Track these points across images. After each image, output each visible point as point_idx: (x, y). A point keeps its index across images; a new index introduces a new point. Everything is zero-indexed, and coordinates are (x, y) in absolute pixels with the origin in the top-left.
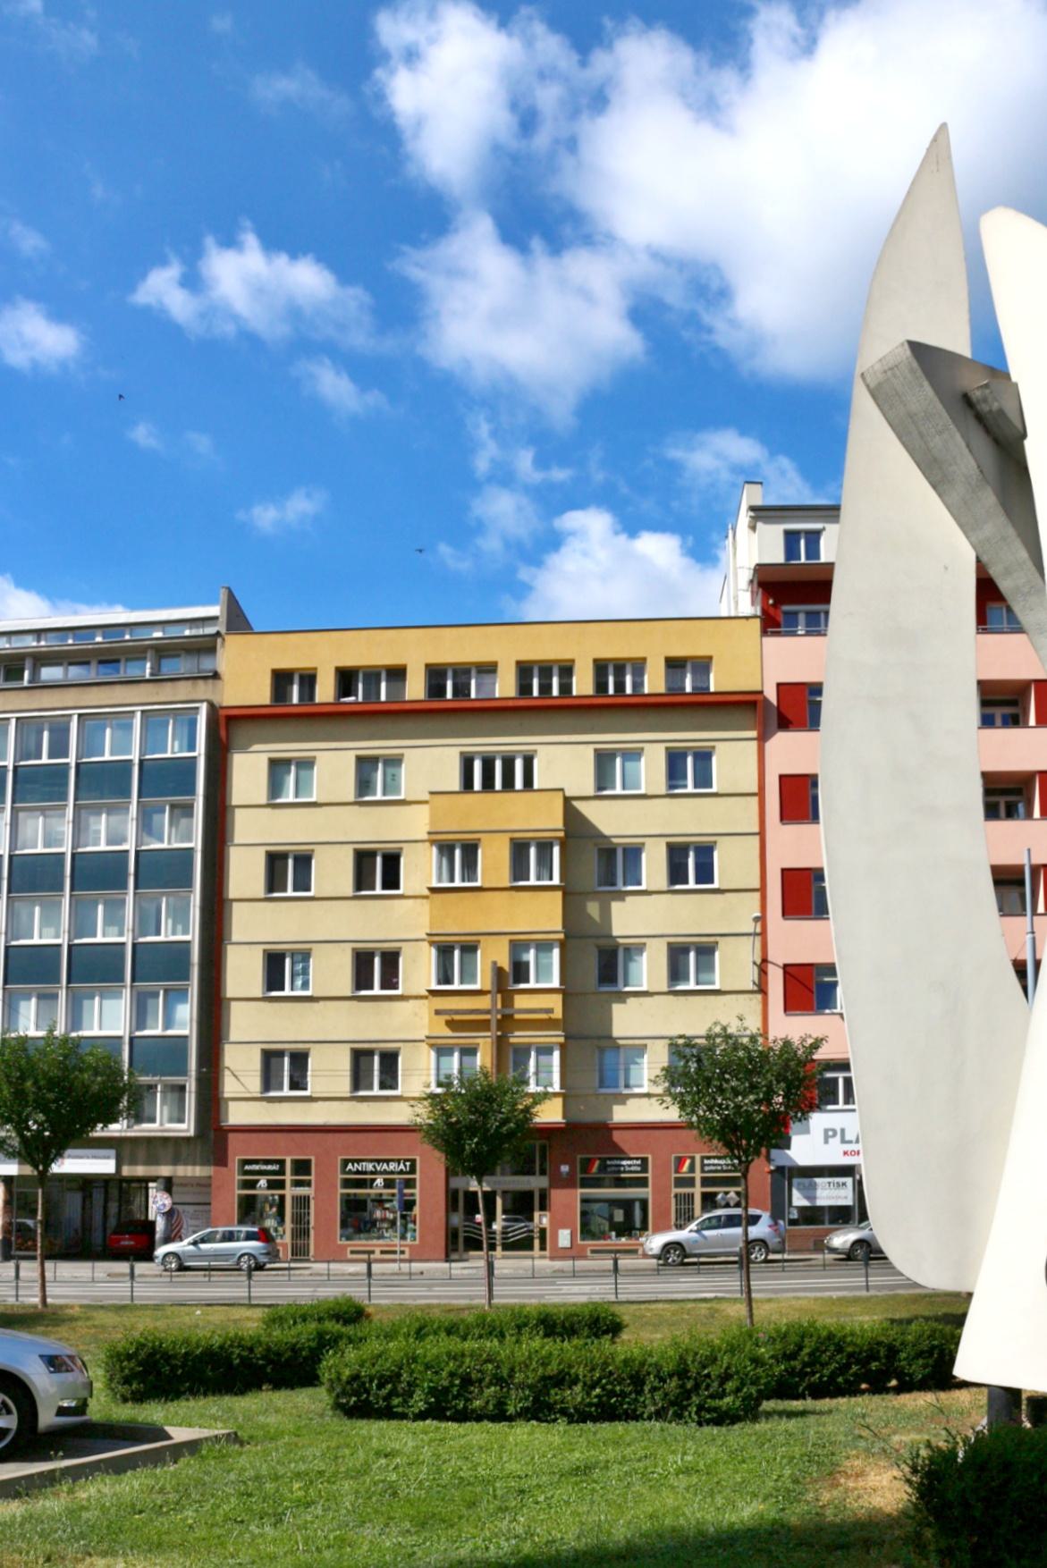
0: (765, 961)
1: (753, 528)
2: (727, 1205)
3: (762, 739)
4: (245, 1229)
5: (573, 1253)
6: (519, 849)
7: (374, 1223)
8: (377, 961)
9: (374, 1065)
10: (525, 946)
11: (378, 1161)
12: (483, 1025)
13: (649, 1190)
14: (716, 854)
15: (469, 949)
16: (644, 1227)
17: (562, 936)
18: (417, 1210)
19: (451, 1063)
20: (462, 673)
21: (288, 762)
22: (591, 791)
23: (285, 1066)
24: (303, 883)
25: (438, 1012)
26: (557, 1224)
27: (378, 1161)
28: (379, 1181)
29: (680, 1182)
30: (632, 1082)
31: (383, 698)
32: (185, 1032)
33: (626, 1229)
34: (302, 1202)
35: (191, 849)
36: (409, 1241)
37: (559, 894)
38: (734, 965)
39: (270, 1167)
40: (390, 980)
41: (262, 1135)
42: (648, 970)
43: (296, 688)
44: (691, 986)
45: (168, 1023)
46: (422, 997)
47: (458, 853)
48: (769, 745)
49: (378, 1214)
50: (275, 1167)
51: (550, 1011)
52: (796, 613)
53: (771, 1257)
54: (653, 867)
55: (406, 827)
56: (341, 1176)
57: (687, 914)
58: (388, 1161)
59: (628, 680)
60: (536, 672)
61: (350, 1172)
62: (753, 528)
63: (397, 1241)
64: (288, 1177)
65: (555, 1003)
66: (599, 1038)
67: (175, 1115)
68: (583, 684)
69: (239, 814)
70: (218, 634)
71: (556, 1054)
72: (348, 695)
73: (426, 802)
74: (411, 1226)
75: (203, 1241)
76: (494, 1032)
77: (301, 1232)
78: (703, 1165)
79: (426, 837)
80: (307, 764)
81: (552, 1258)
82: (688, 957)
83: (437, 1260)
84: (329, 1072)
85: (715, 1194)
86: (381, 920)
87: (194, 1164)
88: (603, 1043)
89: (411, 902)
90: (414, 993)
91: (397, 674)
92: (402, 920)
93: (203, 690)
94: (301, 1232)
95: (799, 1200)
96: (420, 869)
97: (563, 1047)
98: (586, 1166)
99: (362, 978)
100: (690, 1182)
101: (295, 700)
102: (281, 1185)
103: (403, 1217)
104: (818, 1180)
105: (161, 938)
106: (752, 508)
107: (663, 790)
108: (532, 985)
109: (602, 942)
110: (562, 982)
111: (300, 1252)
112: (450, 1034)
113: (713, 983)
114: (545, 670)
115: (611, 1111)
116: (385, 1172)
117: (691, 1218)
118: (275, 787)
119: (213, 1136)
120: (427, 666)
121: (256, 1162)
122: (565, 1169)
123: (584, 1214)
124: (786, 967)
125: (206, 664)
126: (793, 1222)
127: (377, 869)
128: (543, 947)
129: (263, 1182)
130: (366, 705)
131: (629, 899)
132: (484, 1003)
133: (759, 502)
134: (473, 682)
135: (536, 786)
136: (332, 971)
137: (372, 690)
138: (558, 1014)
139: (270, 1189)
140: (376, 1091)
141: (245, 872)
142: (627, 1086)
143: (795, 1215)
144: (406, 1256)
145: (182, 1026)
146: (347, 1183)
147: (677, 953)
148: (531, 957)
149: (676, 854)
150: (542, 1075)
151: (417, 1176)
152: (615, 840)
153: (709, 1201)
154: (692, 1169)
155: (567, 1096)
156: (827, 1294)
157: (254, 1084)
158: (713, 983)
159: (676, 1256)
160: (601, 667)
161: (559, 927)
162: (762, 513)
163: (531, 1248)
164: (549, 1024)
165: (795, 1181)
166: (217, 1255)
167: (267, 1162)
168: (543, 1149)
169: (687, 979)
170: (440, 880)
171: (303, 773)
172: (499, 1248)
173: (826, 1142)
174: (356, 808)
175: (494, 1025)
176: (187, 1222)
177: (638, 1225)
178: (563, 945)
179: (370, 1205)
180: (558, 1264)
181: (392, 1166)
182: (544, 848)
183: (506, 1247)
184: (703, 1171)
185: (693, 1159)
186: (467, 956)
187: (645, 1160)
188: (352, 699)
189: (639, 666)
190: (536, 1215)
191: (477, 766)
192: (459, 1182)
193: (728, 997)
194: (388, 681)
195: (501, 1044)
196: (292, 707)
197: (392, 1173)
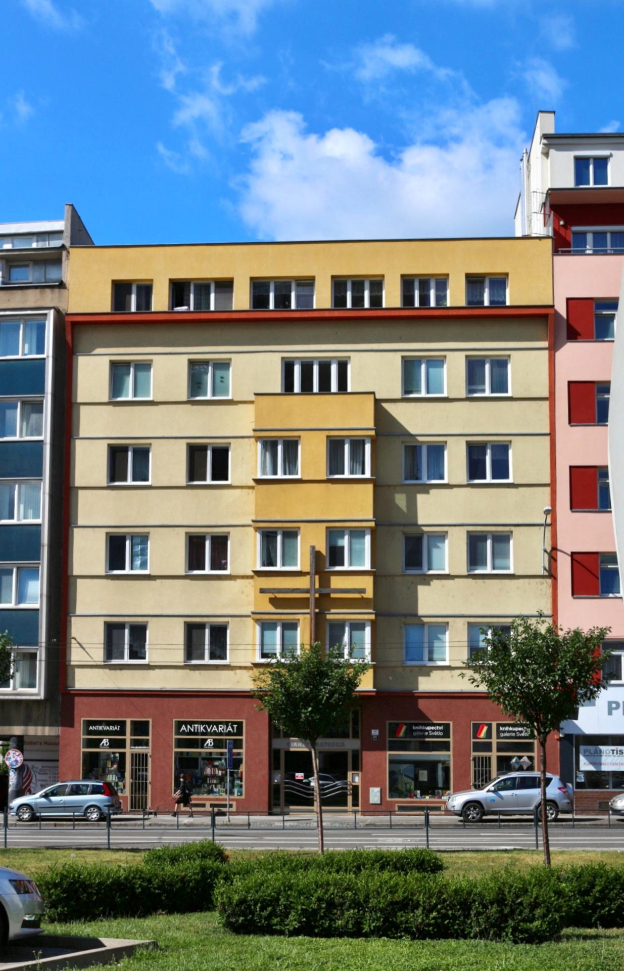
0: (554, 549)
1: (546, 154)
2: (521, 769)
3: (553, 349)
4: (90, 783)
5: (383, 808)
6: (335, 446)
7: (204, 779)
9: (205, 638)
10: (340, 533)
11: (209, 723)
12: (302, 603)
13: (451, 753)
14: (510, 452)
15: (291, 535)
16: (446, 787)
17: (373, 524)
18: (243, 768)
19: (274, 638)
20: (283, 286)
21: (127, 364)
22: (398, 394)
24: (141, 473)
25: (262, 591)
26: (368, 783)
28: (209, 742)
29: (478, 747)
30: (435, 656)
31: (212, 308)
32: (37, 606)
33: (430, 788)
34: (140, 760)
35: (41, 442)
36: (236, 796)
37: (370, 487)
38: (526, 552)
39: (111, 728)
40: (219, 562)
42: (450, 555)
43: (134, 298)
44: (488, 570)
45: (21, 598)
46: (247, 577)
47: (280, 448)
48: (559, 355)
49: (208, 771)
51: (363, 591)
52: (584, 234)
53: (560, 816)
54: (455, 463)
55: (234, 425)
57: (485, 506)
58: (217, 724)
59: (432, 293)
60: (349, 285)
61: (184, 733)
62: (546, 154)
63: (227, 797)
64: (128, 737)
65: (367, 583)
66: (405, 616)
67: (27, 681)
68: (391, 298)
69: (83, 410)
70: (63, 247)
71: (368, 630)
72: (182, 305)
73: (252, 402)
74: (237, 782)
75: (54, 793)
76: (312, 609)
77: (139, 787)
78: (498, 732)
79: (252, 433)
80: (144, 366)
81: (364, 813)
82: (483, 544)
83: (261, 813)
84: (165, 643)
85: (511, 758)
86: (210, 508)
87: (44, 725)
88: (410, 620)
89: (238, 491)
91: (225, 286)
92: (232, 507)
93: (50, 298)
94: (139, 787)
95: (585, 765)
96: (246, 462)
97: (373, 624)
98: (394, 730)
99: (195, 560)
100: (487, 747)
101: (133, 309)
102: (122, 744)
103: (232, 774)
104: (602, 748)
105: (14, 521)
106: (545, 136)
108: (346, 567)
109: (410, 530)
110: (373, 565)
112: (273, 610)
113: (508, 568)
114: (358, 284)
116: (215, 733)
117: (487, 779)
118: (116, 386)
119: (61, 699)
122: (375, 732)
123: (392, 773)
124: (573, 555)
125: (53, 274)
126: (579, 785)
127: (208, 462)
128: (357, 534)
130: (195, 314)
131: (433, 492)
132: (303, 583)
133: (551, 131)
134: (293, 295)
135: (349, 390)
137: (202, 302)
138: (369, 594)
139: (109, 746)
140: (207, 661)
141: (90, 463)
142: (431, 659)
143: (582, 779)
144: (234, 809)
145: (34, 600)
146: (180, 743)
147: (475, 543)
148: (345, 542)
149: (475, 453)
151: (244, 737)
152: (420, 439)
153: (504, 764)
156: (612, 849)
157: (98, 655)
158: (508, 568)
159: (476, 815)
160: (407, 282)
161: (371, 517)
163: (345, 804)
164: (361, 603)
165: (582, 748)
166: (65, 807)
167: (108, 723)
168: (356, 713)
169: (484, 564)
170: (264, 473)
171: (141, 375)
172: (317, 804)
173: (610, 713)
174: (189, 406)
175: (312, 602)
176: (36, 778)
177: (440, 785)
178: (373, 532)
179: (201, 762)
180: (369, 819)
181: (221, 728)
182: (357, 445)
184: (498, 737)
185: (490, 726)
187: (447, 727)
188: (184, 308)
189: (442, 282)
190: (350, 774)
191: (297, 369)
192: (278, 743)
193: (521, 581)
194: (215, 293)
195: (319, 621)
196: (129, 314)
197: (221, 734)
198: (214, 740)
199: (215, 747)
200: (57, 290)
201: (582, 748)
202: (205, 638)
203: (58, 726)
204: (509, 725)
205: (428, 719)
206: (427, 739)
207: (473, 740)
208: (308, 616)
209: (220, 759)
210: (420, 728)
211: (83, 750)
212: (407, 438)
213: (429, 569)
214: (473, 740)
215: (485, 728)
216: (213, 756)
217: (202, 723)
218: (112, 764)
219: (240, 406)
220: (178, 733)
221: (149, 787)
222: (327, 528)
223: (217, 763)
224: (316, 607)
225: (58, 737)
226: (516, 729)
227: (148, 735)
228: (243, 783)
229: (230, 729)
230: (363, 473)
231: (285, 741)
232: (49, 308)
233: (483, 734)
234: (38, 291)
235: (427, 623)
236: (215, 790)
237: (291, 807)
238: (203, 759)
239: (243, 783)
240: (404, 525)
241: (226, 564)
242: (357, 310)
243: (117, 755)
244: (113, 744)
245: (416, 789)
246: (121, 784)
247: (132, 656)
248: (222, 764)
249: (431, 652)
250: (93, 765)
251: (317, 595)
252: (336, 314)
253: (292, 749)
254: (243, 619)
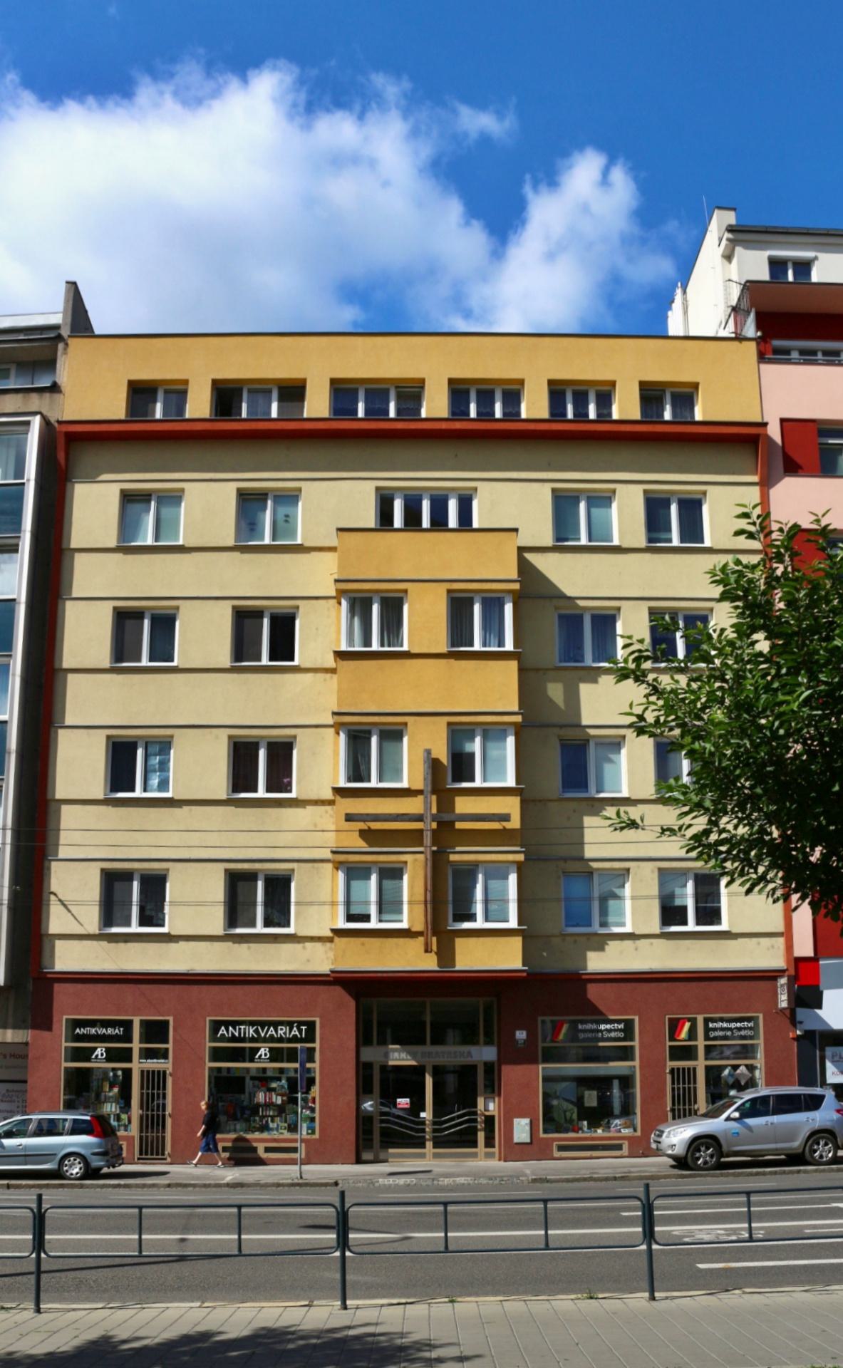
3: (766, 484)
6: (459, 607)
7: (255, 1109)
8: (262, 754)
9: (257, 894)
11: (263, 1024)
12: (414, 838)
15: (392, 735)
18: (316, 1091)
20: (377, 391)
22: (548, 539)
23: (133, 893)
24: (162, 649)
25: (349, 818)
26: (511, 1114)
27: (263, 1024)
30: (611, 919)
37: (513, 665)
39: (110, 1031)
40: (279, 779)
41: (100, 987)
47: (375, 608)
49: (261, 1097)
50: (117, 1031)
51: (506, 818)
55: (307, 580)
56: (209, 1045)
58: (276, 1025)
61: (223, 1039)
63: (287, 1135)
64: (136, 1045)
65: (512, 806)
68: (534, 406)
69: (79, 559)
77: (153, 1121)
78: (707, 1030)
84: (195, 902)
86: (264, 701)
88: (572, 866)
89: (309, 676)
90: (313, 796)
91: (293, 392)
92: (300, 700)
94: (153, 1121)
96: (323, 632)
97: (520, 868)
99: (242, 777)
100: (687, 1053)
102: (126, 1056)
107: (641, 542)
108: (478, 783)
109: (569, 733)
110: (518, 782)
111: (151, 1149)
115: (585, 959)
116: (272, 1039)
118: (127, 525)
120: (334, 382)
121: (92, 1023)
122: (521, 1035)
127: (264, 635)
128: (492, 733)
129: (100, 1051)
132: (413, 806)
136: (200, 767)
138: (515, 823)
140: (260, 929)
146: (217, 1055)
148: (476, 746)
150: (493, 907)
151: (317, 1045)
152: (581, 603)
154: (692, 1034)
155: (528, 933)
157: (91, 919)
162: (741, 235)
164: (504, 837)
168: (488, 1010)
171: (166, 511)
172: (429, 1144)
174: (237, 555)
175: (428, 839)
177: (617, 1110)
178: (519, 731)
181: (282, 1031)
182: (493, 606)
184: (707, 1038)
185: (694, 1022)
186: (389, 746)
187: (629, 1025)
190: (480, 1101)
192: (369, 1054)
194: (280, 400)
195: (438, 863)
197: (280, 1040)
198: (271, 1049)
199: (272, 1060)
200: (47, 395)
201: (829, 1051)
202: (257, 894)
203: (26, 1028)
204: (722, 1020)
205: (601, 1013)
206: (601, 1044)
207: (669, 1044)
208: (421, 857)
209: (279, 1079)
210: (589, 1026)
211: (65, 1065)
212: (562, 603)
213: (598, 792)
214: (669, 1044)
215: (687, 1025)
216: (269, 1074)
217: (252, 1023)
218: (111, 1087)
219: (314, 554)
220: (214, 1037)
221: (169, 1121)
222: (449, 724)
223: (274, 1085)
224: (433, 844)
225: (27, 1044)
226: (733, 1025)
227: (166, 1041)
228: (317, 1115)
229: (295, 1032)
230: (501, 643)
231: (382, 1049)
232: (34, 414)
233: (684, 1035)
234: (20, 396)
235: (598, 869)
236: (271, 1125)
237: (391, 1151)
238: (253, 1078)
239: (317, 1115)
240: (561, 726)
241: (290, 784)
242: (484, 427)
243: (120, 1073)
244: (112, 1056)
245: (581, 1118)
246: (124, 1116)
247: (143, 922)
248: (282, 1087)
249: (604, 912)
250: (81, 1087)
251: (434, 825)
252: (458, 425)
253: (391, 1063)
254: (316, 865)
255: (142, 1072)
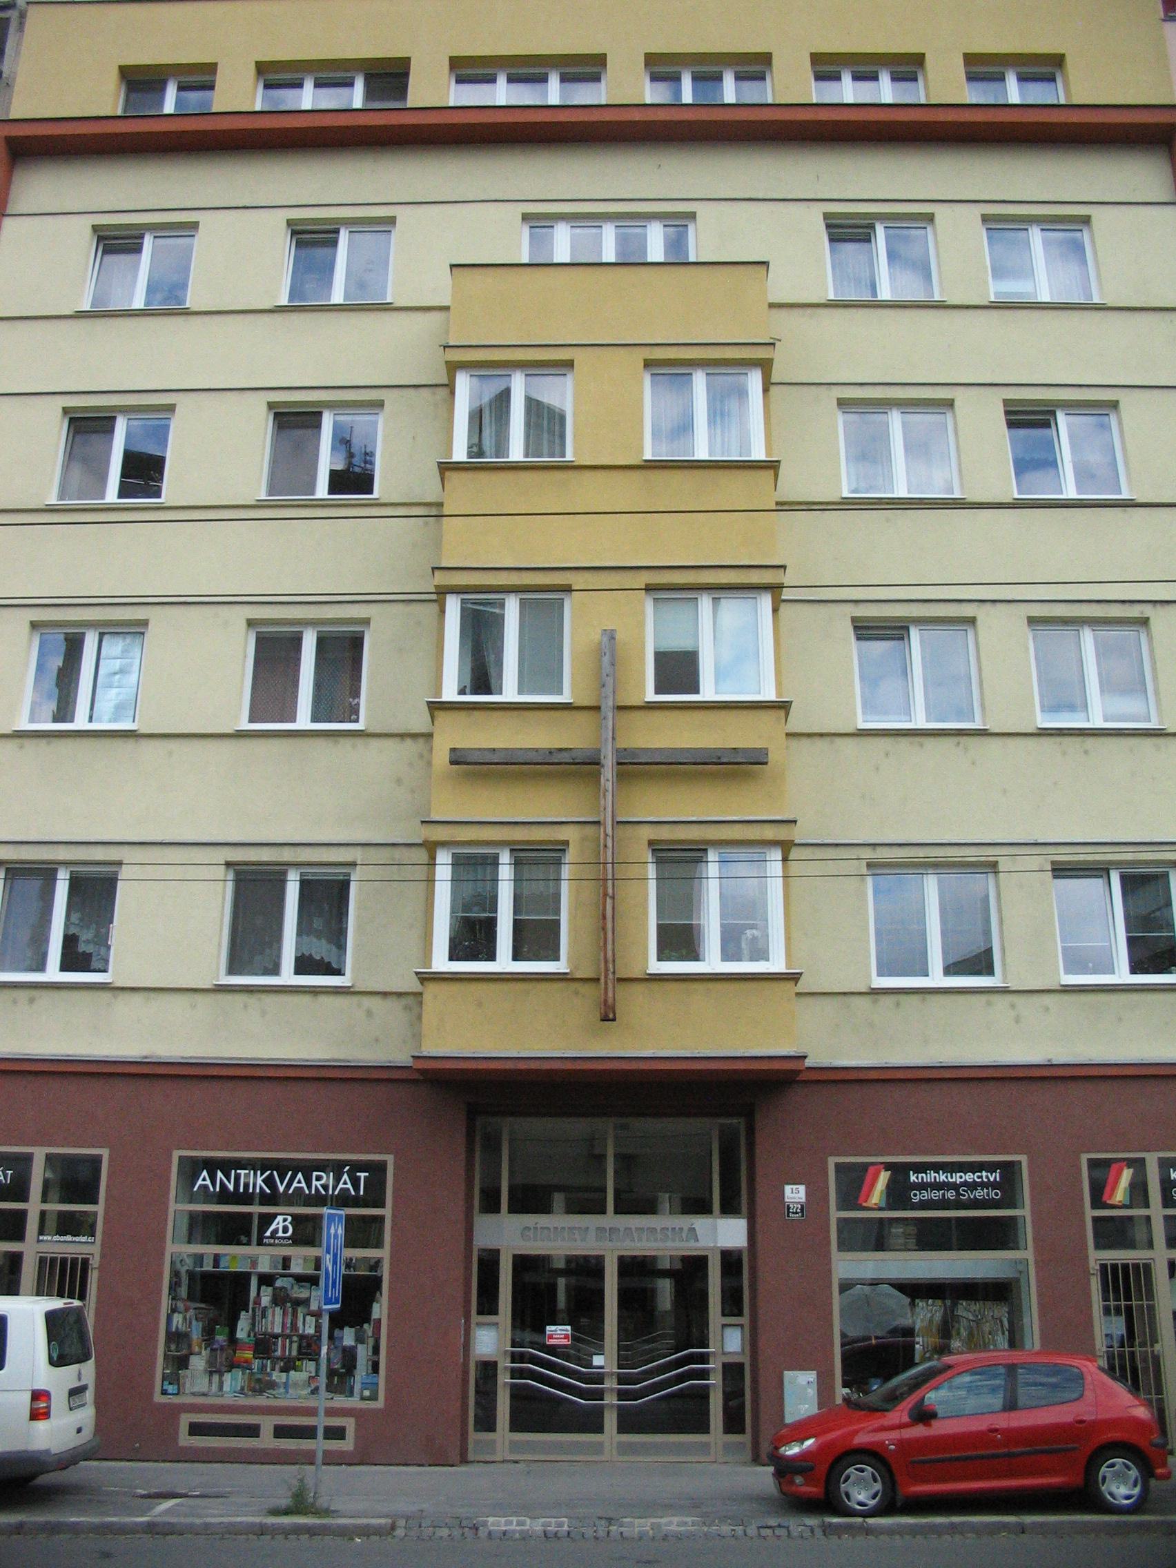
11: (282, 1167)
13: (1027, 1254)
58: (307, 1169)
64: (33, 1206)
98: (853, 1183)
122: (795, 1194)
144: (347, 1445)
146: (202, 1227)
151: (387, 1212)
154: (1139, 1191)
181: (322, 1181)
183: (628, 1423)
198: (297, 1219)
215: (1127, 1175)
217: (263, 1165)
229: (345, 1183)
255: (42, 1261)
